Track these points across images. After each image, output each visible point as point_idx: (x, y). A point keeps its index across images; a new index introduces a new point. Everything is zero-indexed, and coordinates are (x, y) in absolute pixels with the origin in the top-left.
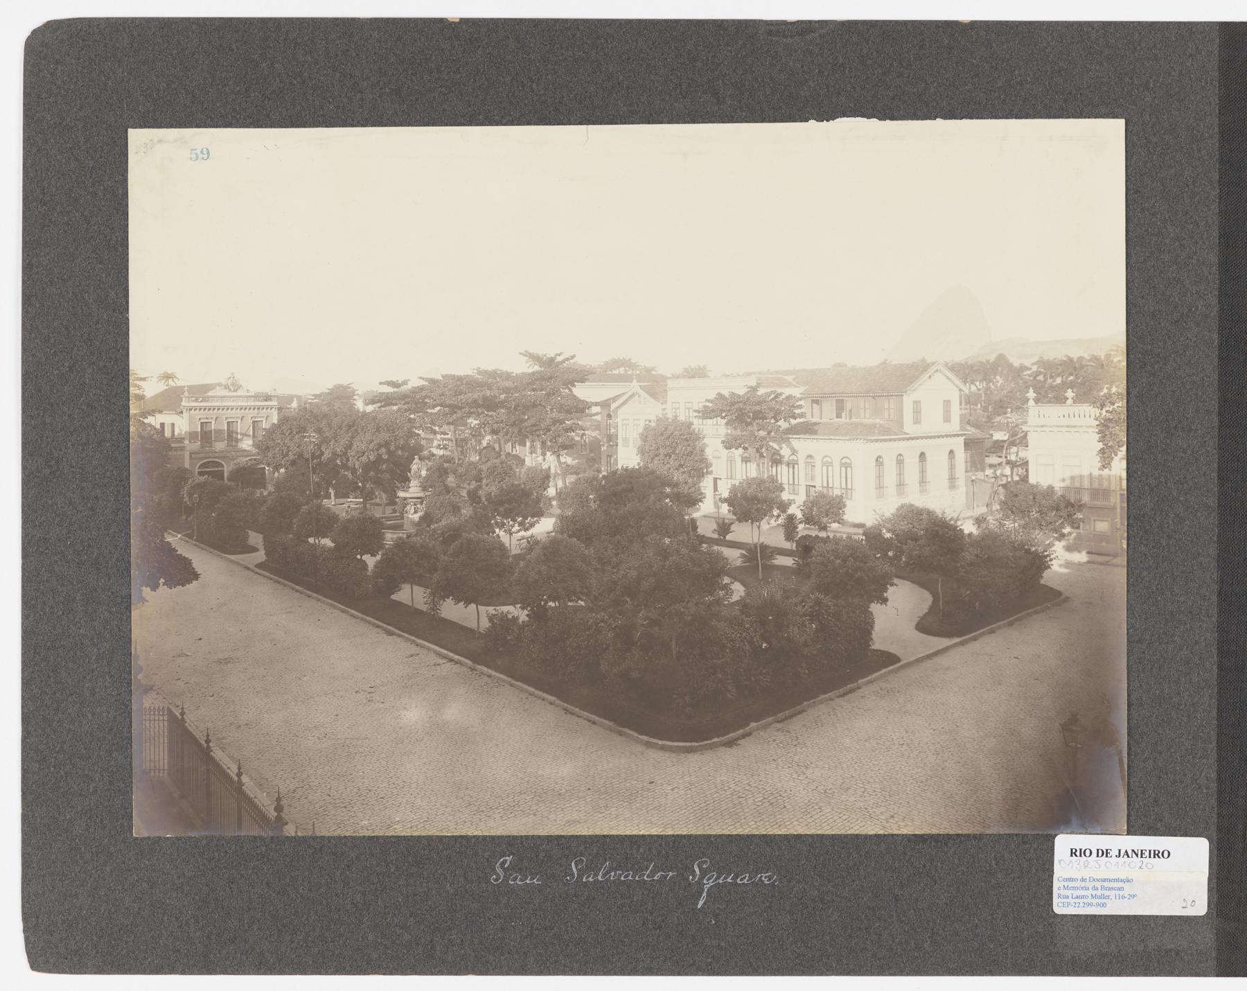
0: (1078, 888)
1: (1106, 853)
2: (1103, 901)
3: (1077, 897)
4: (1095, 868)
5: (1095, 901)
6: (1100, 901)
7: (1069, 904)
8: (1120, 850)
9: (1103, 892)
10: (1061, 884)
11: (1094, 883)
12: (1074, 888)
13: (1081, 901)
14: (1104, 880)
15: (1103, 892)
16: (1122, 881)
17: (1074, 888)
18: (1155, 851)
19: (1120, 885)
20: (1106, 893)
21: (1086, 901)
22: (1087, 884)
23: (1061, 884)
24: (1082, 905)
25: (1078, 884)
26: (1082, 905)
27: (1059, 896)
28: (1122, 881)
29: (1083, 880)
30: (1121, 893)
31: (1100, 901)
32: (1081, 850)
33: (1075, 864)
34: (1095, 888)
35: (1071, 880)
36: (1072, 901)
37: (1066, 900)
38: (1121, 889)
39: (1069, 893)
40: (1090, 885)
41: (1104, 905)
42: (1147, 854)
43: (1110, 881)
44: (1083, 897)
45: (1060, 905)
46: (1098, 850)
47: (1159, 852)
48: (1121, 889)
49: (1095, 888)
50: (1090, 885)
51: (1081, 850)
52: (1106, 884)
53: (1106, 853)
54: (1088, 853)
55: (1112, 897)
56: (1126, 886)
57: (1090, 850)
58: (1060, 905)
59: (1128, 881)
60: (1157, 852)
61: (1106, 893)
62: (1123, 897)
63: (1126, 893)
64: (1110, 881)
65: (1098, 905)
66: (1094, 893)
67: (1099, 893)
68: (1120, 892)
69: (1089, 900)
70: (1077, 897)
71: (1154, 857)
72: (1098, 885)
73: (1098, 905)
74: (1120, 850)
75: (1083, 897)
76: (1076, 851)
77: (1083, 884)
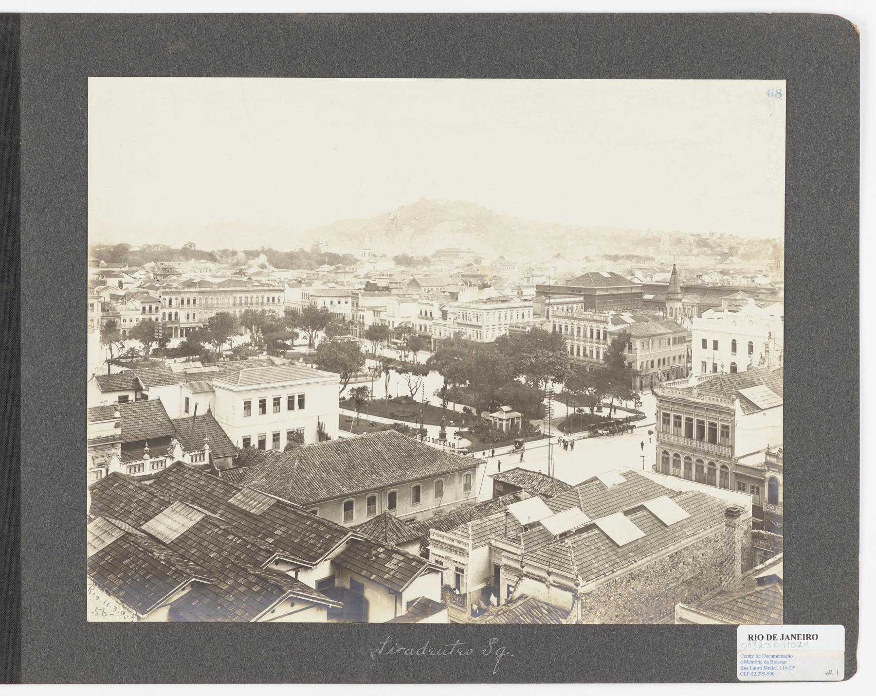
0: (755, 662)
1: (773, 637)
2: (772, 671)
3: (754, 668)
4: (766, 648)
5: (766, 671)
6: (770, 671)
7: (748, 673)
8: (783, 635)
9: (772, 665)
10: (743, 659)
11: (766, 659)
12: (752, 662)
13: (757, 671)
14: (773, 656)
15: (772, 665)
16: (785, 657)
17: (752, 662)
18: (807, 635)
19: (784, 659)
20: (774, 665)
21: (759, 671)
22: (761, 659)
23: (743, 659)
24: (757, 674)
25: (755, 659)
26: (757, 674)
27: (741, 668)
28: (785, 657)
29: (758, 656)
30: (785, 665)
31: (770, 671)
32: (756, 635)
33: (752, 645)
34: (766, 662)
35: (750, 656)
36: (750, 671)
37: (744, 671)
38: (783, 662)
39: (748, 665)
40: (763, 660)
41: (772, 674)
42: (802, 637)
43: (777, 657)
44: (758, 668)
45: (742, 674)
46: (768, 635)
47: (810, 635)
48: (783, 662)
49: (766, 662)
50: (763, 660)
51: (756, 635)
52: (775, 659)
53: (773, 637)
54: (761, 637)
55: (779, 668)
56: (788, 660)
57: (763, 636)
58: (742, 674)
59: (789, 657)
60: (809, 636)
61: (774, 665)
62: (786, 668)
63: (787, 665)
64: (777, 657)
65: (769, 674)
66: (766, 665)
67: (769, 665)
68: (781, 665)
69: (763, 670)
70: (754, 668)
71: (807, 639)
72: (769, 659)
73: (769, 674)
74: (783, 635)
75: (758, 668)
76: (752, 636)
77: (758, 659)
